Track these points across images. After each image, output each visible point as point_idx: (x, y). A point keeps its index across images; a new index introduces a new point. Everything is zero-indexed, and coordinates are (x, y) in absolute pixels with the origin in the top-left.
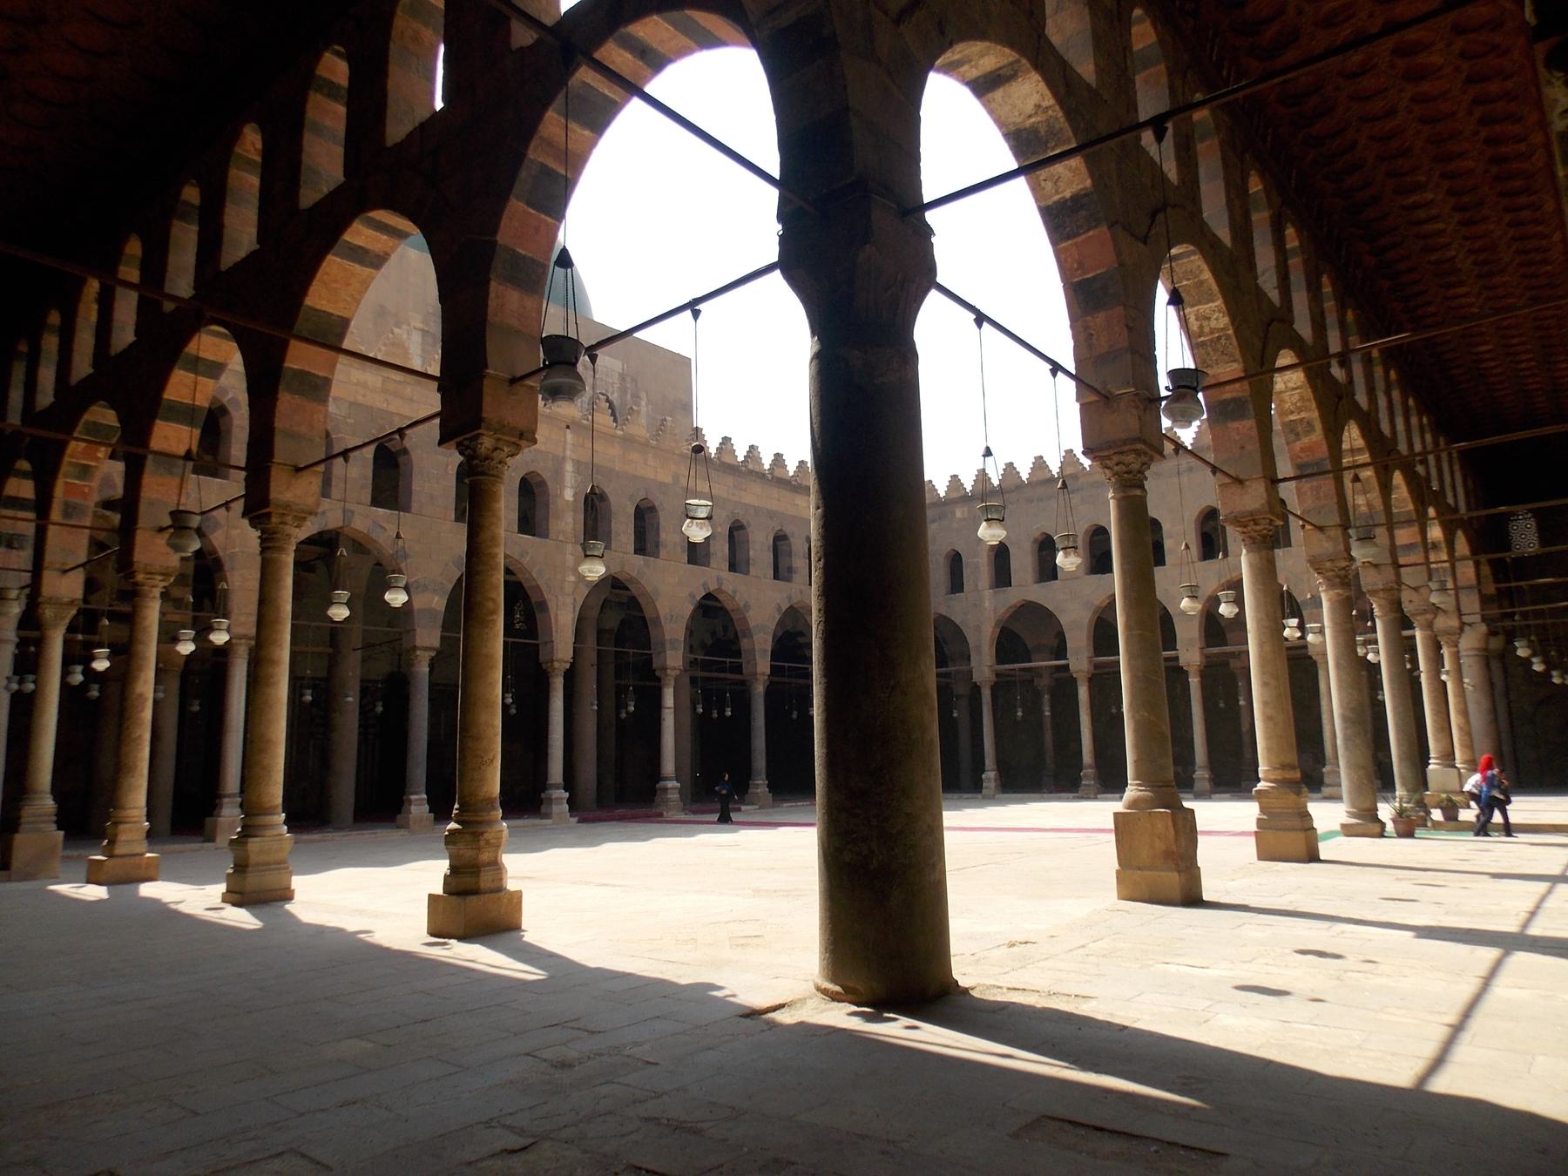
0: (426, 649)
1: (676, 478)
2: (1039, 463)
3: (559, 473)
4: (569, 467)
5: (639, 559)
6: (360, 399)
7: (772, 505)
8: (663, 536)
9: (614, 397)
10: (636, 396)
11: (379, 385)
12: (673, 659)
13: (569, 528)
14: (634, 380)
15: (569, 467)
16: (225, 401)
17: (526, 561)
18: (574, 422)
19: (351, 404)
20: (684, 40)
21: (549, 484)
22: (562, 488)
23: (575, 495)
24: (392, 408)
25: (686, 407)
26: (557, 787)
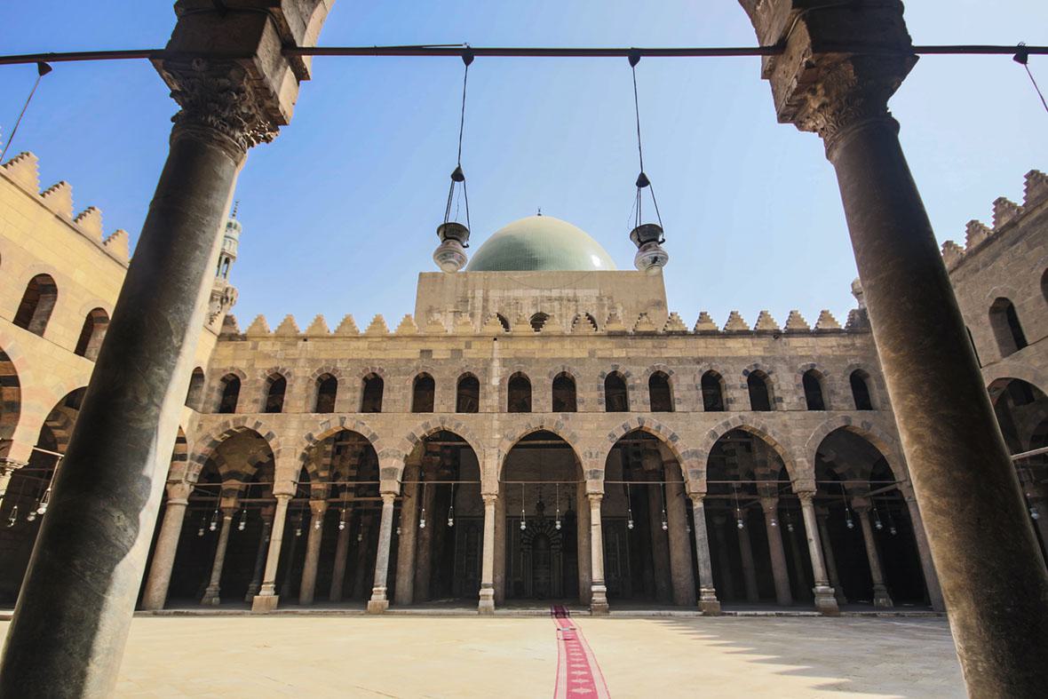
0: (389, 493)
1: (592, 353)
2: (974, 227)
3: (487, 370)
4: (496, 364)
5: (559, 415)
6: (355, 356)
7: (701, 353)
8: (579, 395)
9: (594, 314)
10: (612, 308)
11: (366, 346)
12: (595, 487)
13: (496, 404)
14: (610, 298)
15: (496, 364)
16: (284, 374)
17: (459, 432)
18: (499, 336)
19: (350, 360)
20: (785, 95)
21: (479, 378)
22: (490, 377)
23: (502, 381)
24: (374, 357)
25: (661, 304)
26: (487, 586)
